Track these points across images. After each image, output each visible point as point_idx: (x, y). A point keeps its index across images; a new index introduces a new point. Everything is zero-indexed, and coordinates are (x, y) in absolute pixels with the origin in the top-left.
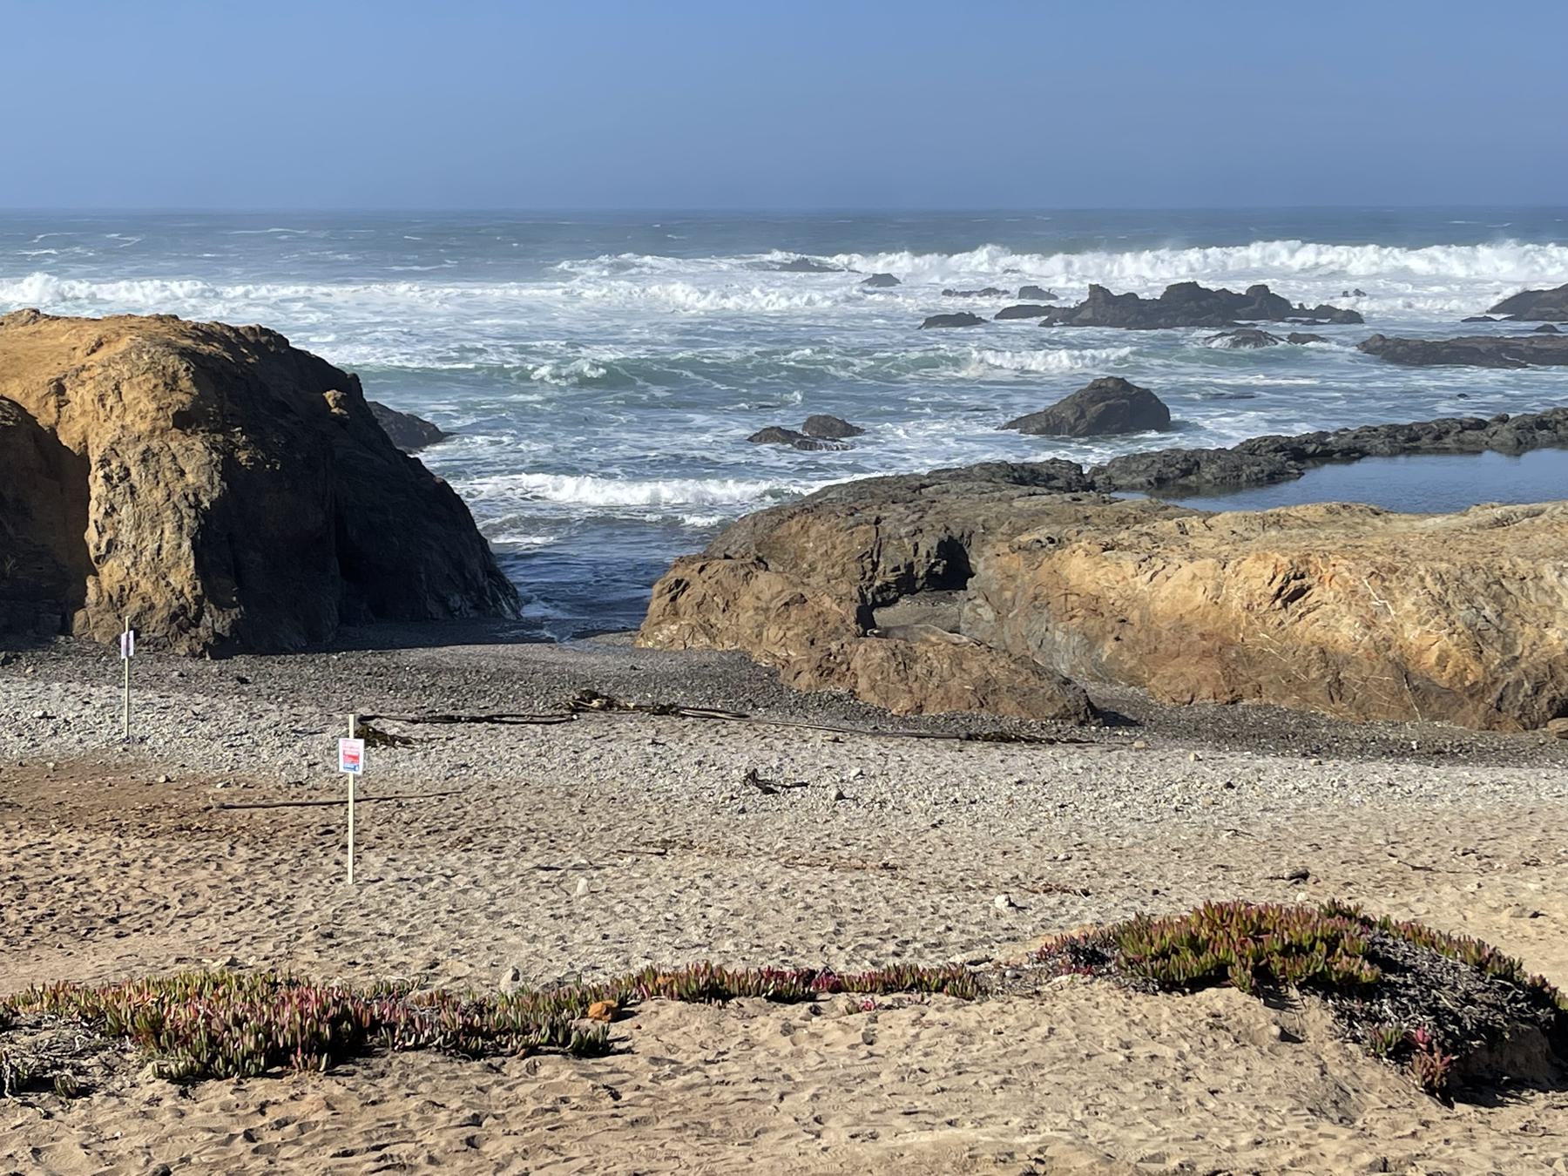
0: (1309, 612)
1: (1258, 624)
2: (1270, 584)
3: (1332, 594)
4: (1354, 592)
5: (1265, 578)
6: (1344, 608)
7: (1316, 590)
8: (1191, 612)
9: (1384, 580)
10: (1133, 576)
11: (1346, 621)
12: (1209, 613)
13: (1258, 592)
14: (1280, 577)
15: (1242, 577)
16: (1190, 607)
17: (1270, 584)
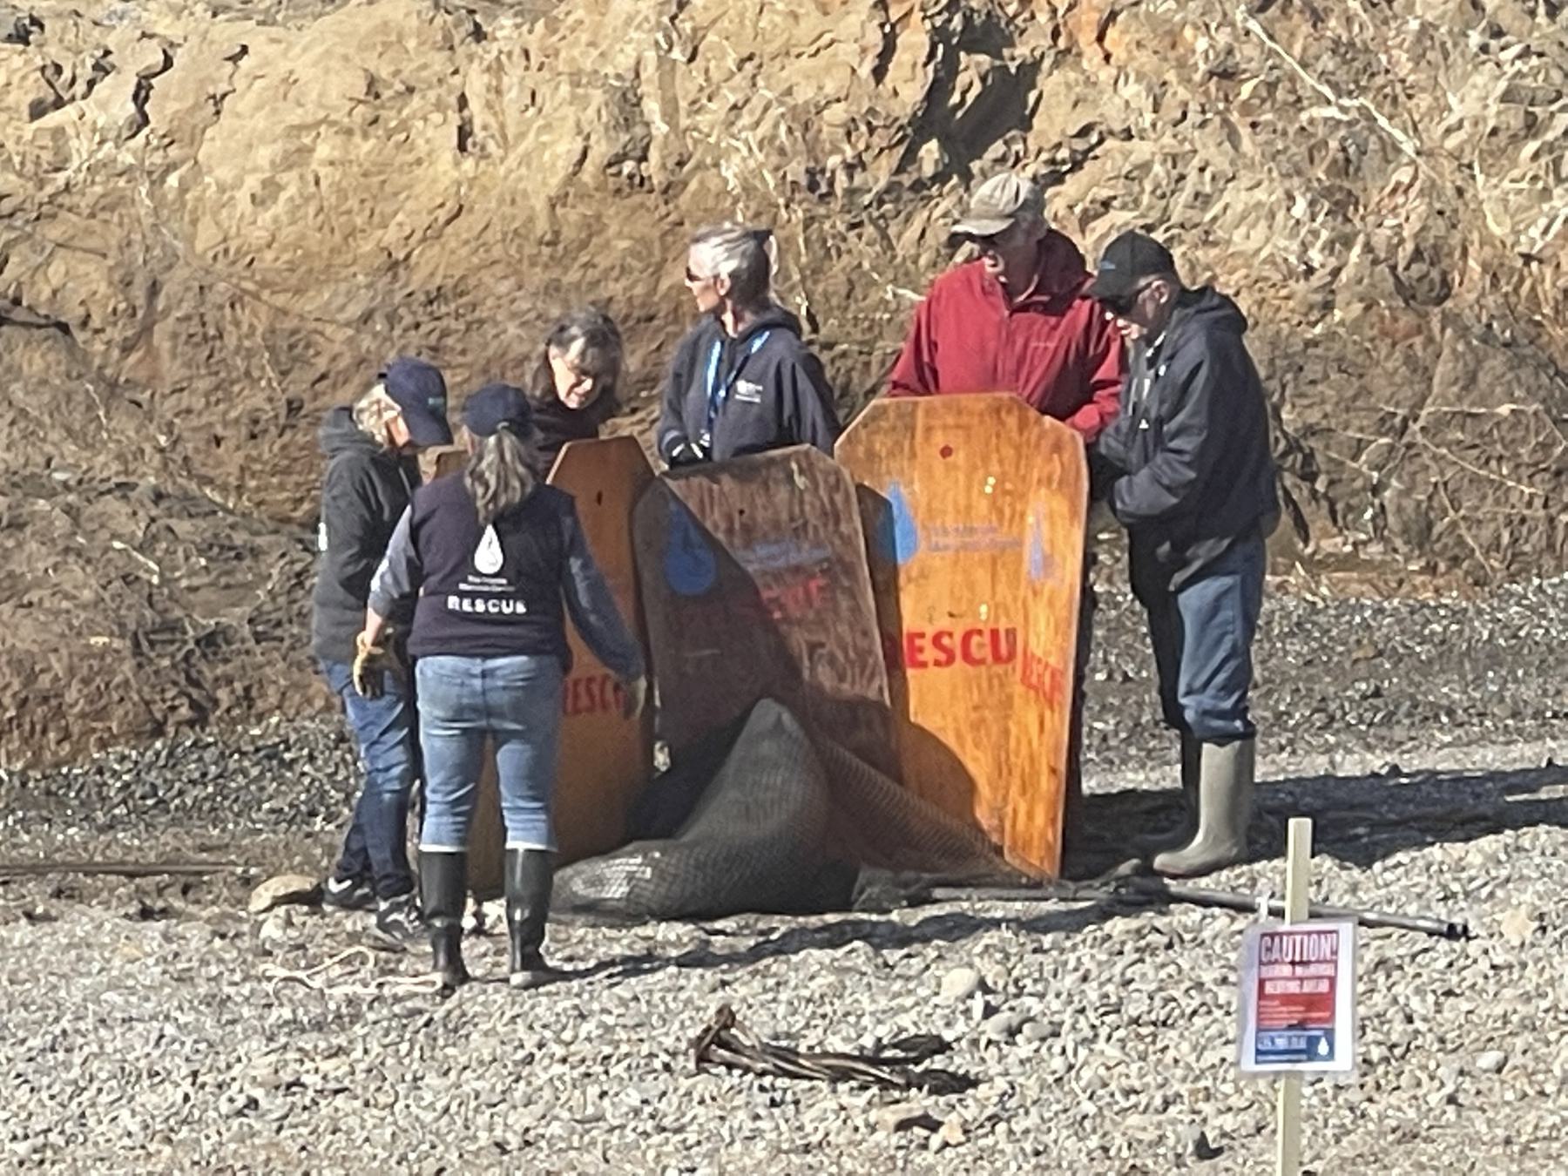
0: (1057, 178)
1: (863, 247)
2: (879, 73)
3: (1131, 90)
4: (1226, 74)
5: (847, 52)
6: (1210, 149)
7: (1050, 83)
8: (433, 234)
9: (1317, 18)
10: (38, 111)
11: (1236, 198)
12: (593, 227)
13: (837, 113)
14: (914, 40)
15: (721, 55)
16: (407, 218)
17: (879, 73)
